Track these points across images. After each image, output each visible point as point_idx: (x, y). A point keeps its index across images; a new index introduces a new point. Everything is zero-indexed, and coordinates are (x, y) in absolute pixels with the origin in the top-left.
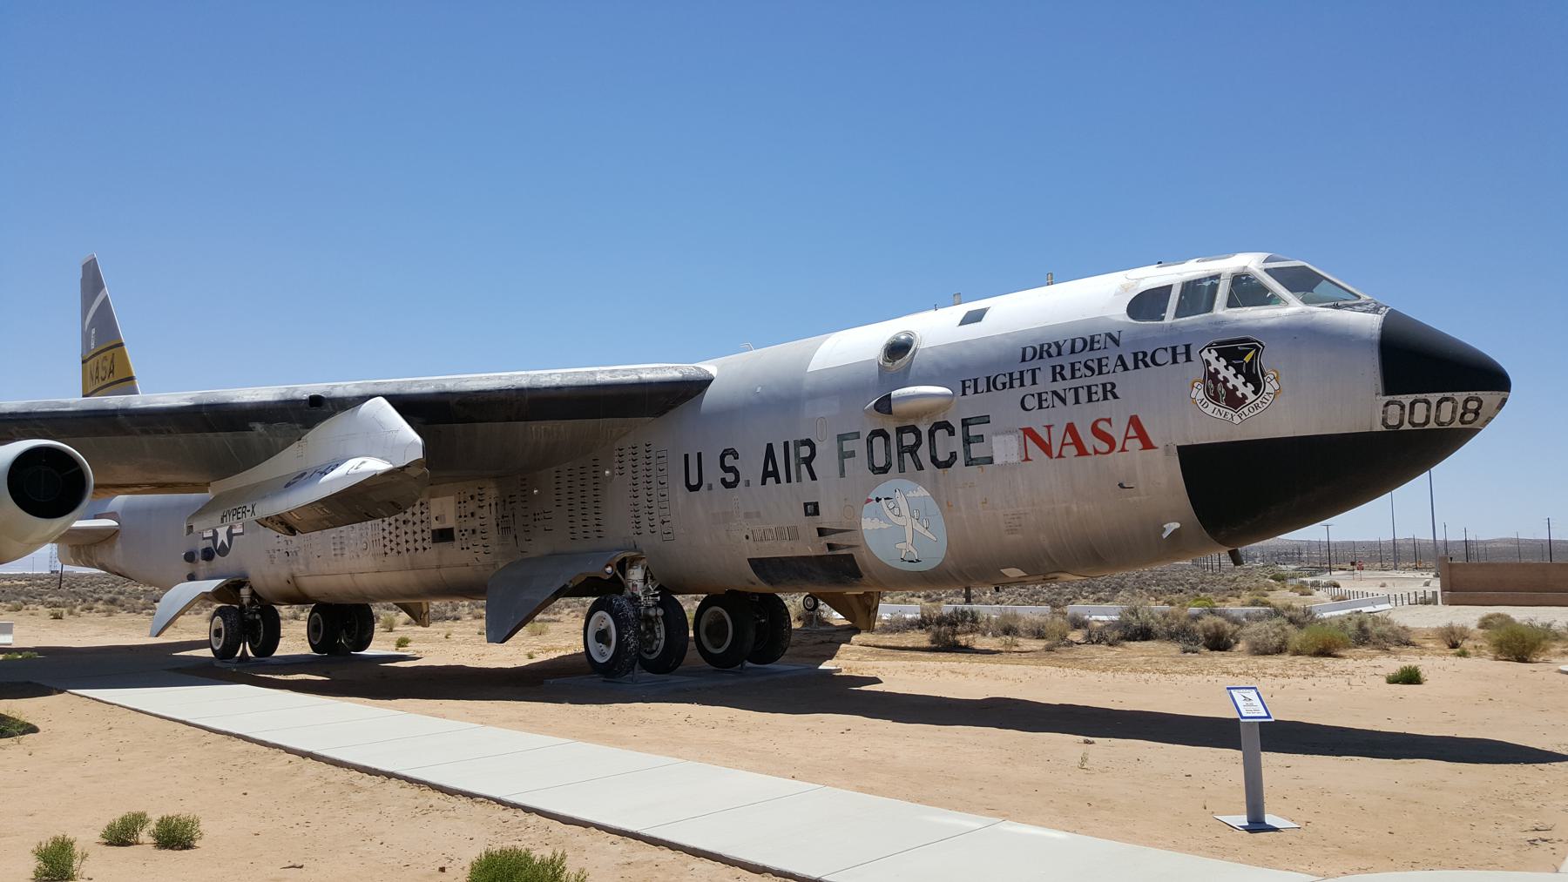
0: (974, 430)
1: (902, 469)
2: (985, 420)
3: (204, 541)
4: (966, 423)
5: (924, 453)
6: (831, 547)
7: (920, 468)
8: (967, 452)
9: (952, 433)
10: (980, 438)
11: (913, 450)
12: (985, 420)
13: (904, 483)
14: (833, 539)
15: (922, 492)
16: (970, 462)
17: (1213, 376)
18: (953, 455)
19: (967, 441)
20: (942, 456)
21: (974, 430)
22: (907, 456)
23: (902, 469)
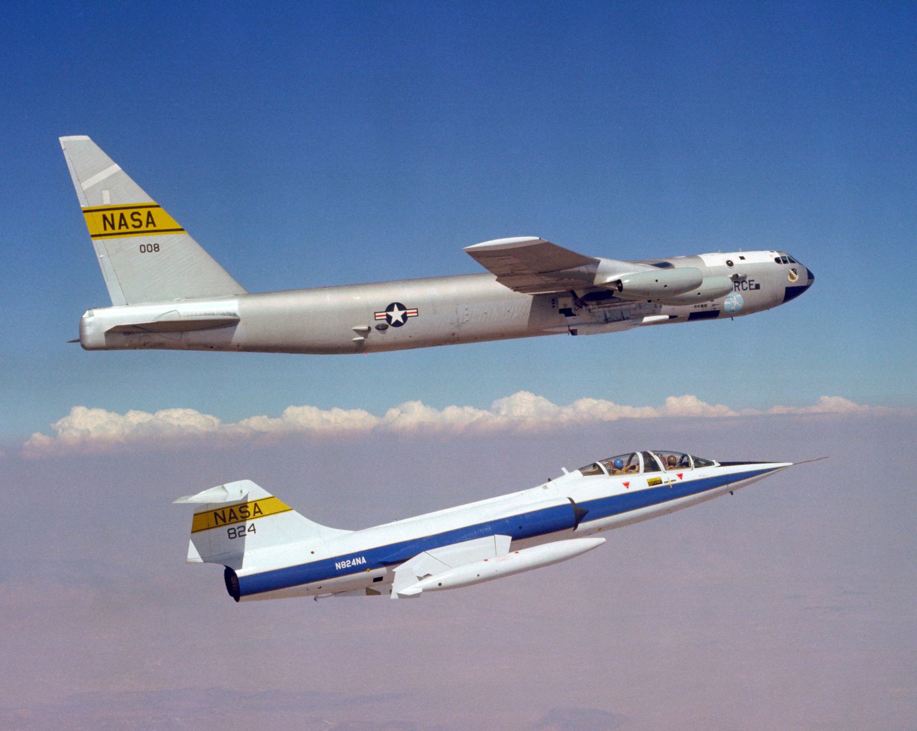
0: (751, 283)
1: (735, 290)
2: (753, 281)
3: (376, 321)
4: (750, 281)
5: (740, 287)
6: (715, 308)
7: (739, 290)
8: (750, 287)
9: (746, 283)
10: (752, 284)
11: (738, 286)
12: (753, 281)
13: (735, 293)
14: (716, 307)
15: (740, 295)
16: (750, 289)
17: (795, 273)
18: (747, 288)
19: (750, 285)
20: (745, 288)
21: (751, 283)
22: (737, 288)
23: (735, 290)
